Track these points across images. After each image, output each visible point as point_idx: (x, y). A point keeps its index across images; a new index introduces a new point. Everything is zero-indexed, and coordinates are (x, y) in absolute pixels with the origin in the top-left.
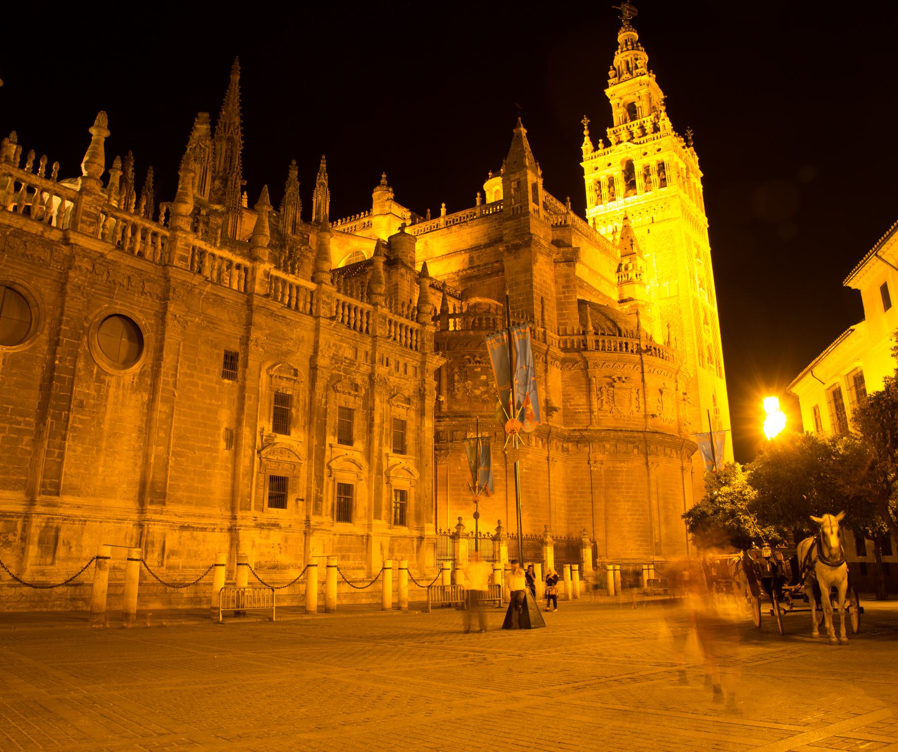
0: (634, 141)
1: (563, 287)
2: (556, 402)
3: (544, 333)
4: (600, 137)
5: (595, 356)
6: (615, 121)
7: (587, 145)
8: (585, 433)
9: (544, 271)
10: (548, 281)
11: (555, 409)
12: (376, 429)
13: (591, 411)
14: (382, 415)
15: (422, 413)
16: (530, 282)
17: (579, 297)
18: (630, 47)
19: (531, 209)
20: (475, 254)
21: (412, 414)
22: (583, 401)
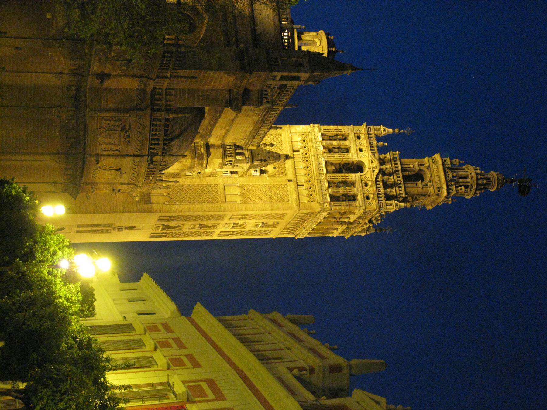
2: (109, 83)
3: (166, 77)
7: (383, 130)
8: (83, 106)
9: (223, 81)
10: (212, 84)
11: (102, 82)
13: (101, 111)
16: (210, 69)
17: (207, 108)
18: (480, 182)
19: (275, 73)
20: (247, 21)
22: (111, 105)
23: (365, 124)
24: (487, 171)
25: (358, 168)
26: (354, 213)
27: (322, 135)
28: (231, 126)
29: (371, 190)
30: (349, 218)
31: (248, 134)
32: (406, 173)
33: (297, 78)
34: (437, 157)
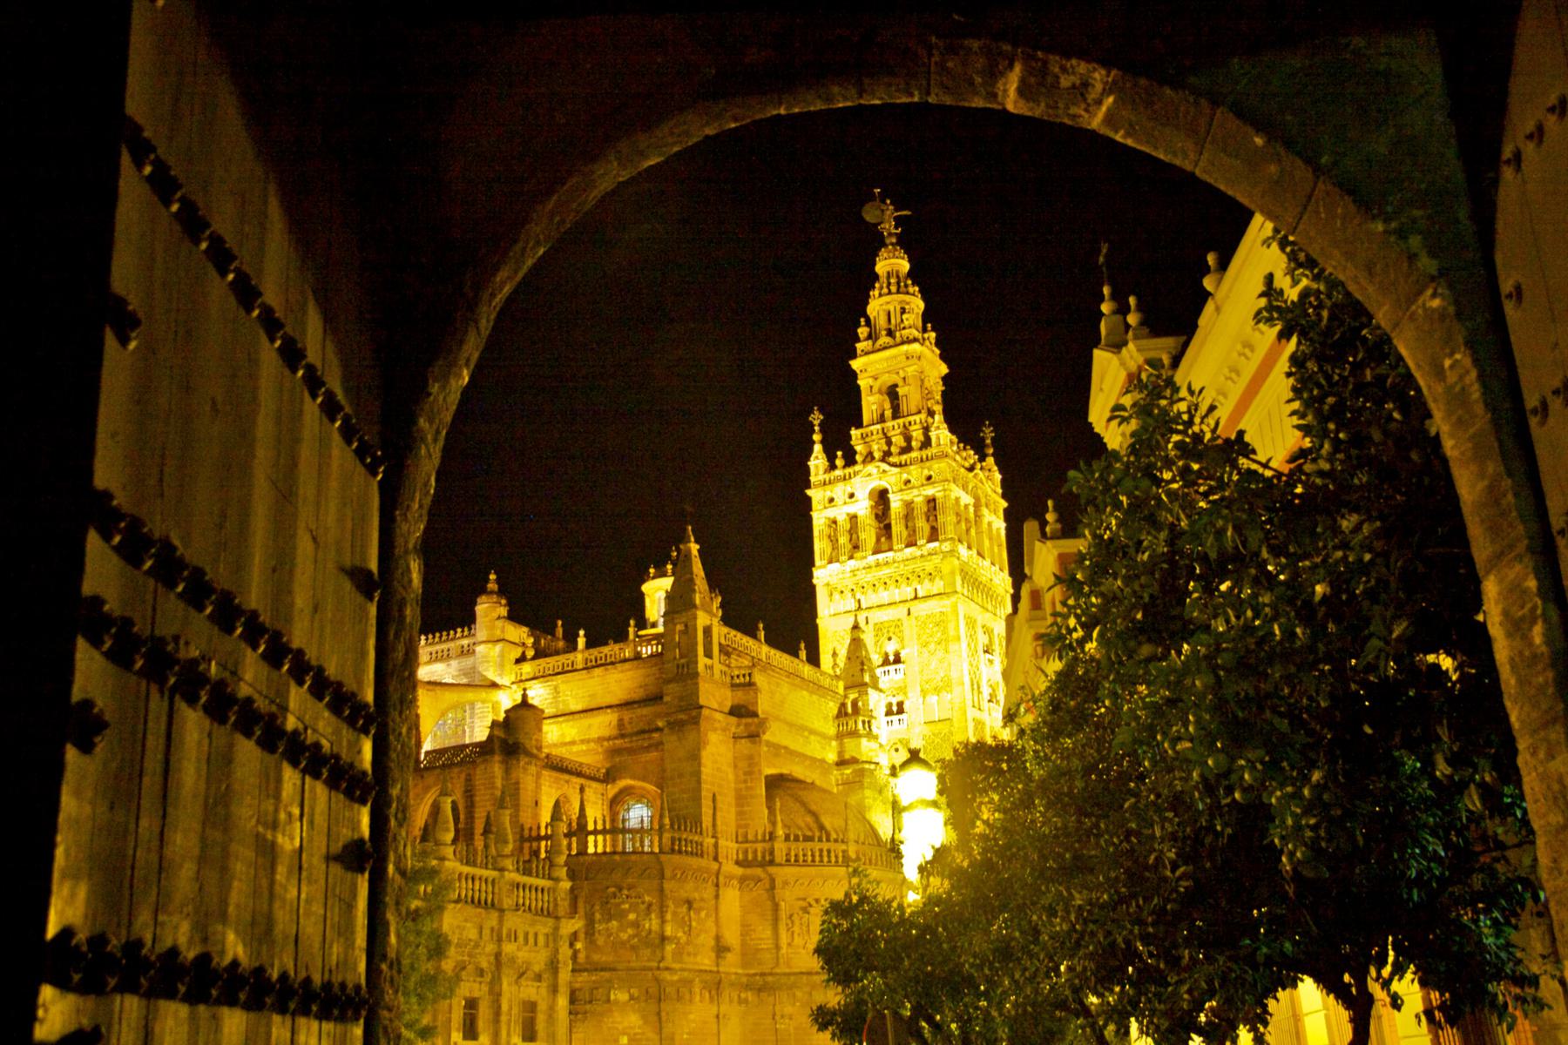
0: (892, 459)
1: (745, 774)
2: (732, 937)
3: (716, 845)
4: (840, 449)
5: (782, 873)
6: (866, 418)
7: (817, 461)
8: (770, 979)
9: (718, 752)
10: (724, 768)
11: (728, 949)
12: (504, 1018)
13: (778, 947)
14: (510, 1001)
15: (554, 990)
16: (697, 774)
18: (893, 289)
20: (627, 715)
21: (544, 991)
22: (769, 933)
23: (809, 492)
24: (876, 277)
25: (882, 497)
26: (957, 499)
27: (830, 562)
28: (803, 728)
29: (915, 473)
30: (966, 506)
31: (815, 697)
32: (888, 413)
33: (708, 631)
34: (856, 364)
